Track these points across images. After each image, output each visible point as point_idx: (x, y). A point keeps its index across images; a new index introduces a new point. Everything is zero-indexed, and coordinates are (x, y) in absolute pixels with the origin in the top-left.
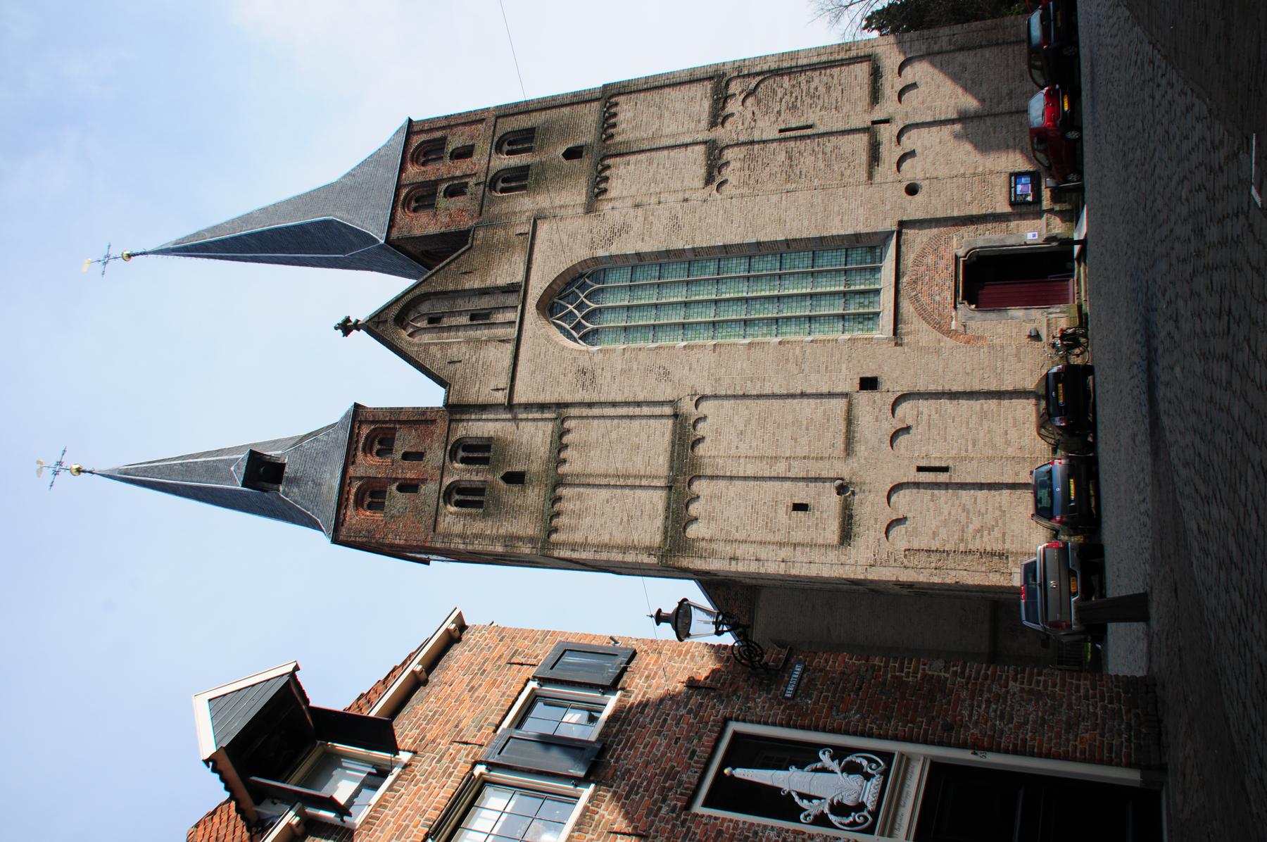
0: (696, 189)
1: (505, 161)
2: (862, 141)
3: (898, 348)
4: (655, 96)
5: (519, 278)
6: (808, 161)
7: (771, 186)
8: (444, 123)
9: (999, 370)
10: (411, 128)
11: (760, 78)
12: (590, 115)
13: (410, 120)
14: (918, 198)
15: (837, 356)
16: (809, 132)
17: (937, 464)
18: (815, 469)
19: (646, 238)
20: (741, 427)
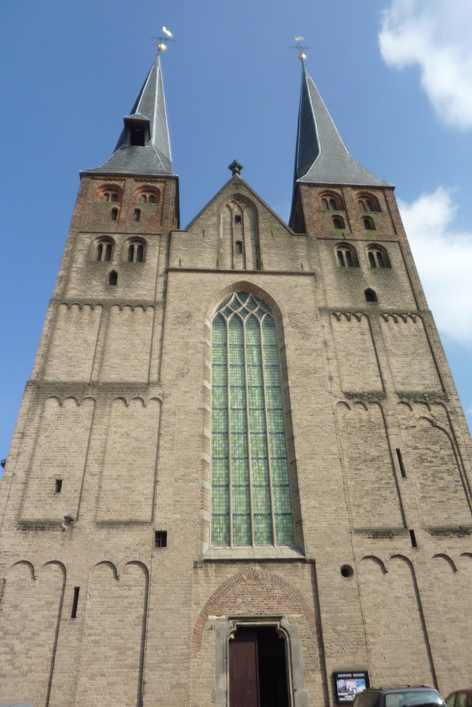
0: (341, 386)
2: (394, 521)
3: (192, 565)
4: (424, 349)
5: (266, 268)
6: (372, 476)
7: (345, 445)
8: (392, 208)
9: (164, 665)
11: (448, 430)
12: (406, 303)
14: (339, 578)
15: (188, 510)
16: (399, 474)
17: (79, 606)
18: (90, 497)
19: (298, 352)
20: (133, 434)
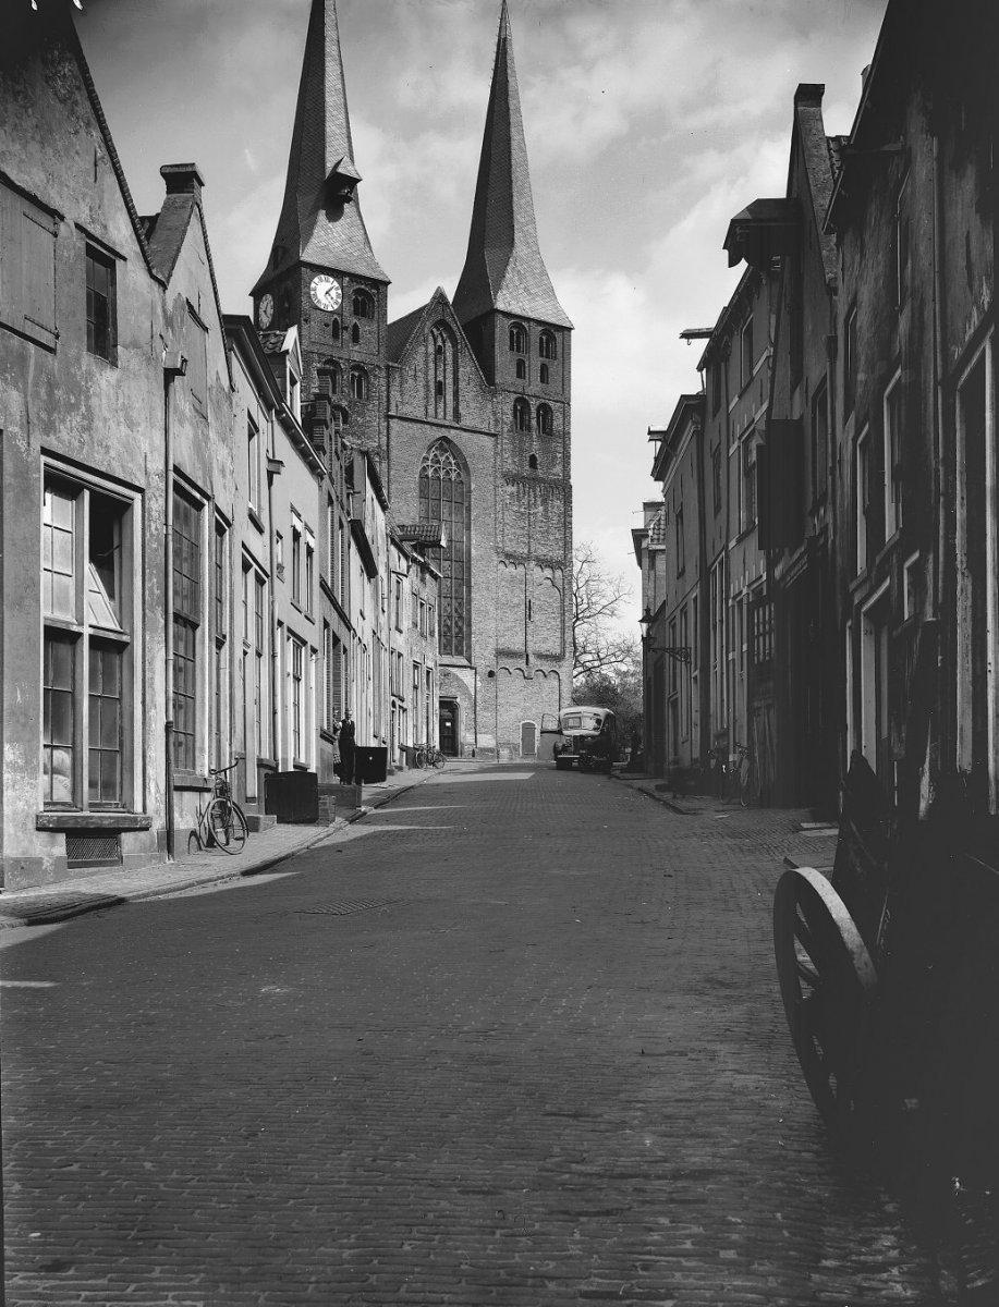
13: (570, 329)
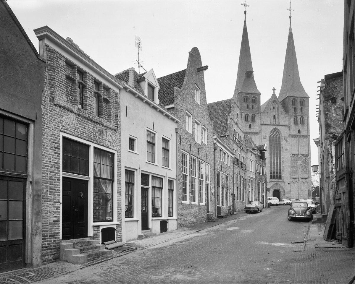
1: (299, 117)
10: (308, 98)
12: (306, 134)
14: (288, 185)
